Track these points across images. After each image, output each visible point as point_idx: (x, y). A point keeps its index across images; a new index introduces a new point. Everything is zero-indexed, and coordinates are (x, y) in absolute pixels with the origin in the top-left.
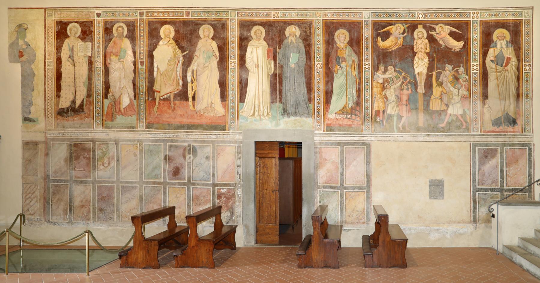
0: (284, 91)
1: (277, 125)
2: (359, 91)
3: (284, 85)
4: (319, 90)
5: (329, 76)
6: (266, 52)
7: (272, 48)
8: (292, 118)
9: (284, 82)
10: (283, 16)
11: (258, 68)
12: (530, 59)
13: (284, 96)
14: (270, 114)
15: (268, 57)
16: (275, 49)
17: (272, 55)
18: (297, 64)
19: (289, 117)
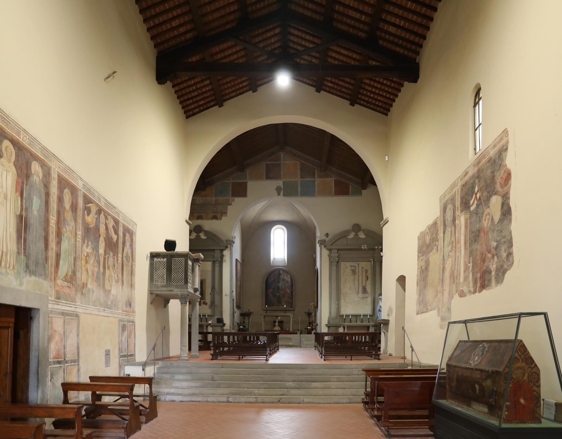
0: (28, 241)
1: (21, 284)
2: (75, 259)
3: (28, 232)
4: (52, 249)
5: (59, 235)
6: (15, 183)
7: (20, 181)
8: (33, 278)
9: (28, 229)
10: (30, 145)
11: (6, 199)
12: (135, 262)
13: (27, 248)
14: (16, 267)
15: (16, 191)
16: (23, 183)
17: (19, 189)
18: (38, 211)
19: (30, 276)
